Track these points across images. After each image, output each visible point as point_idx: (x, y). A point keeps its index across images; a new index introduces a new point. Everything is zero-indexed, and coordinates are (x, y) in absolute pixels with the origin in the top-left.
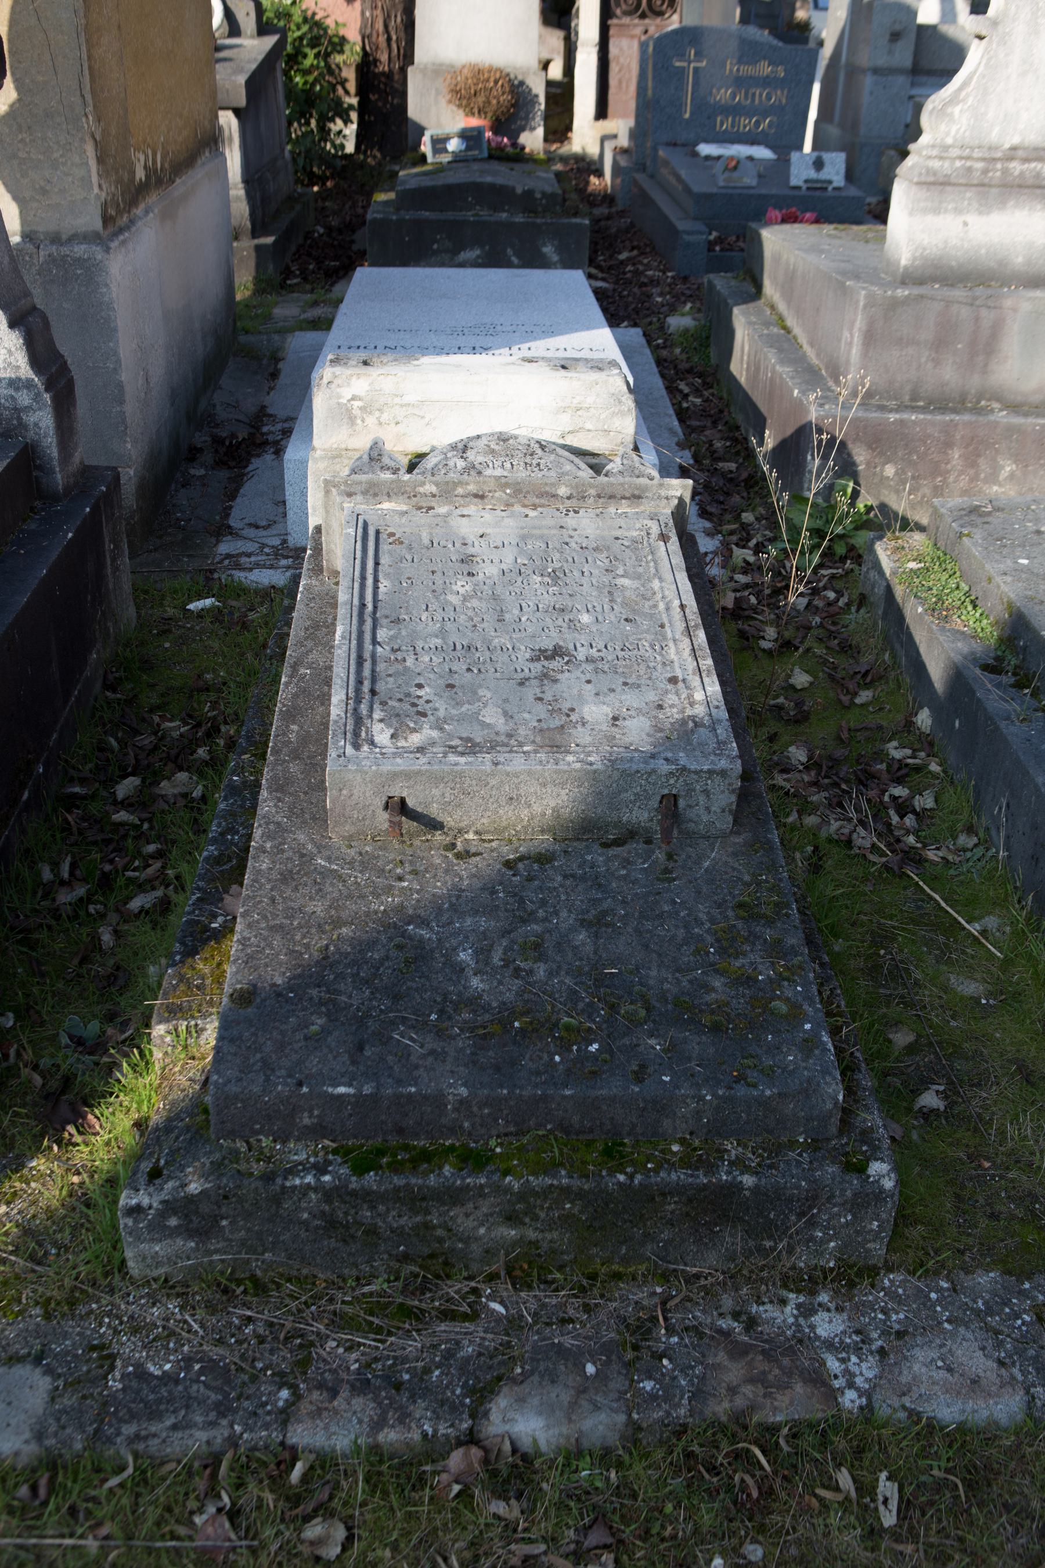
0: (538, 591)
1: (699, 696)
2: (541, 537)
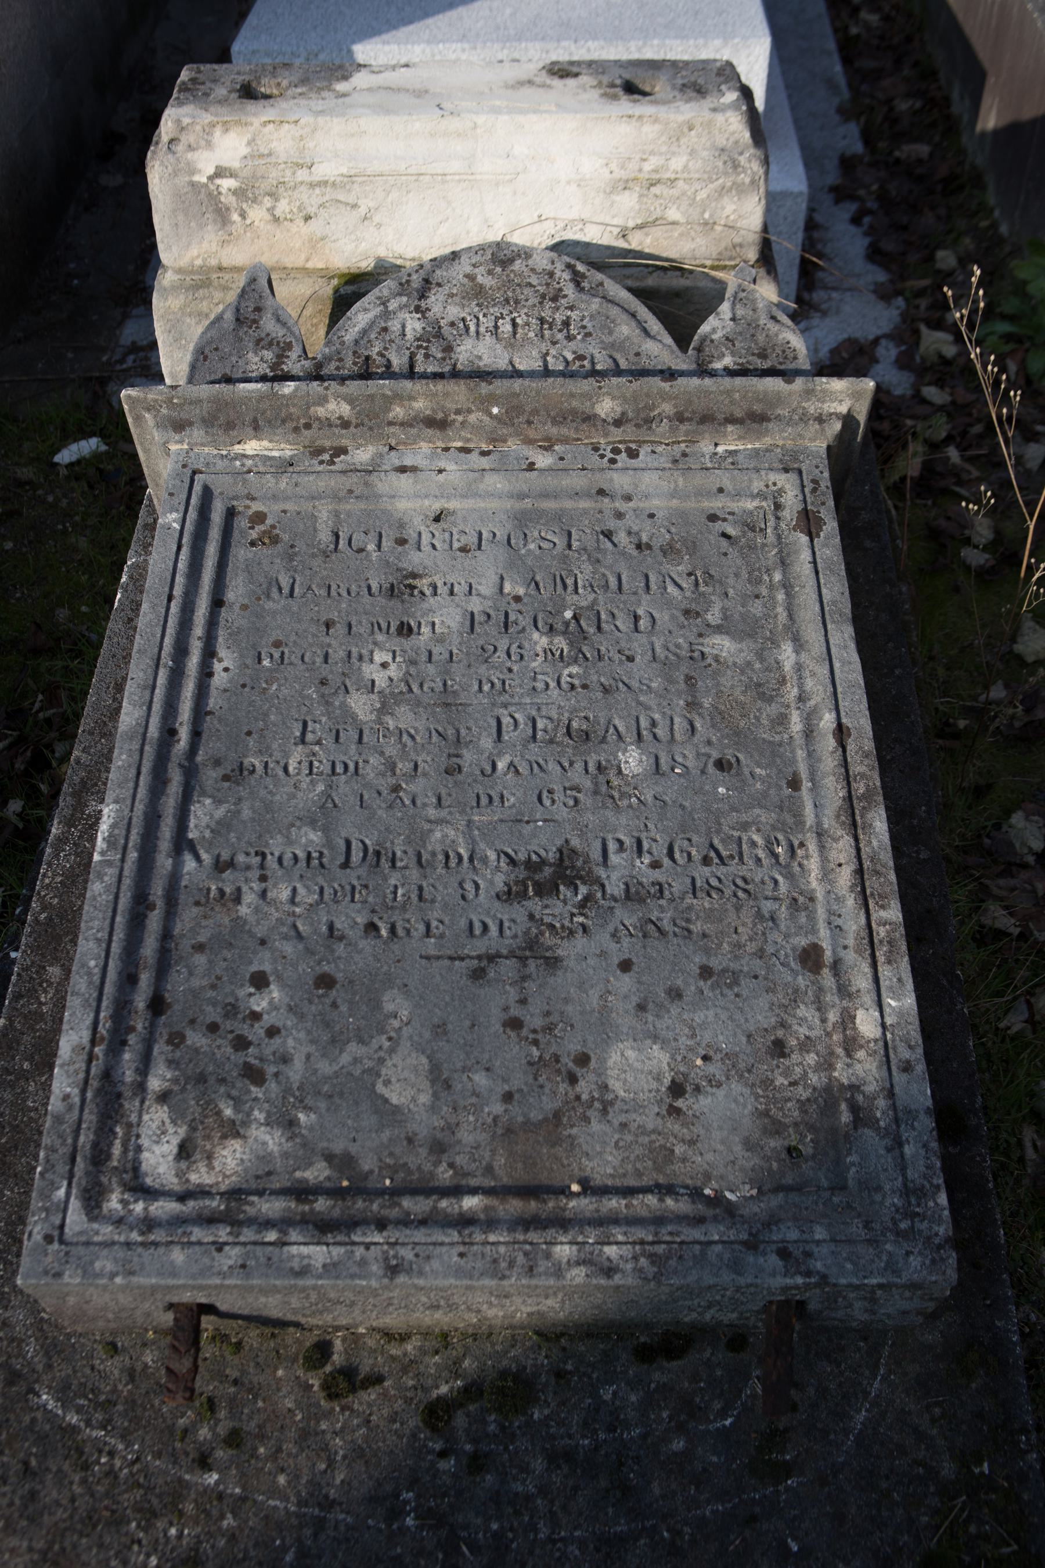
0: (541, 674)
1: (867, 1024)
2: (558, 516)
